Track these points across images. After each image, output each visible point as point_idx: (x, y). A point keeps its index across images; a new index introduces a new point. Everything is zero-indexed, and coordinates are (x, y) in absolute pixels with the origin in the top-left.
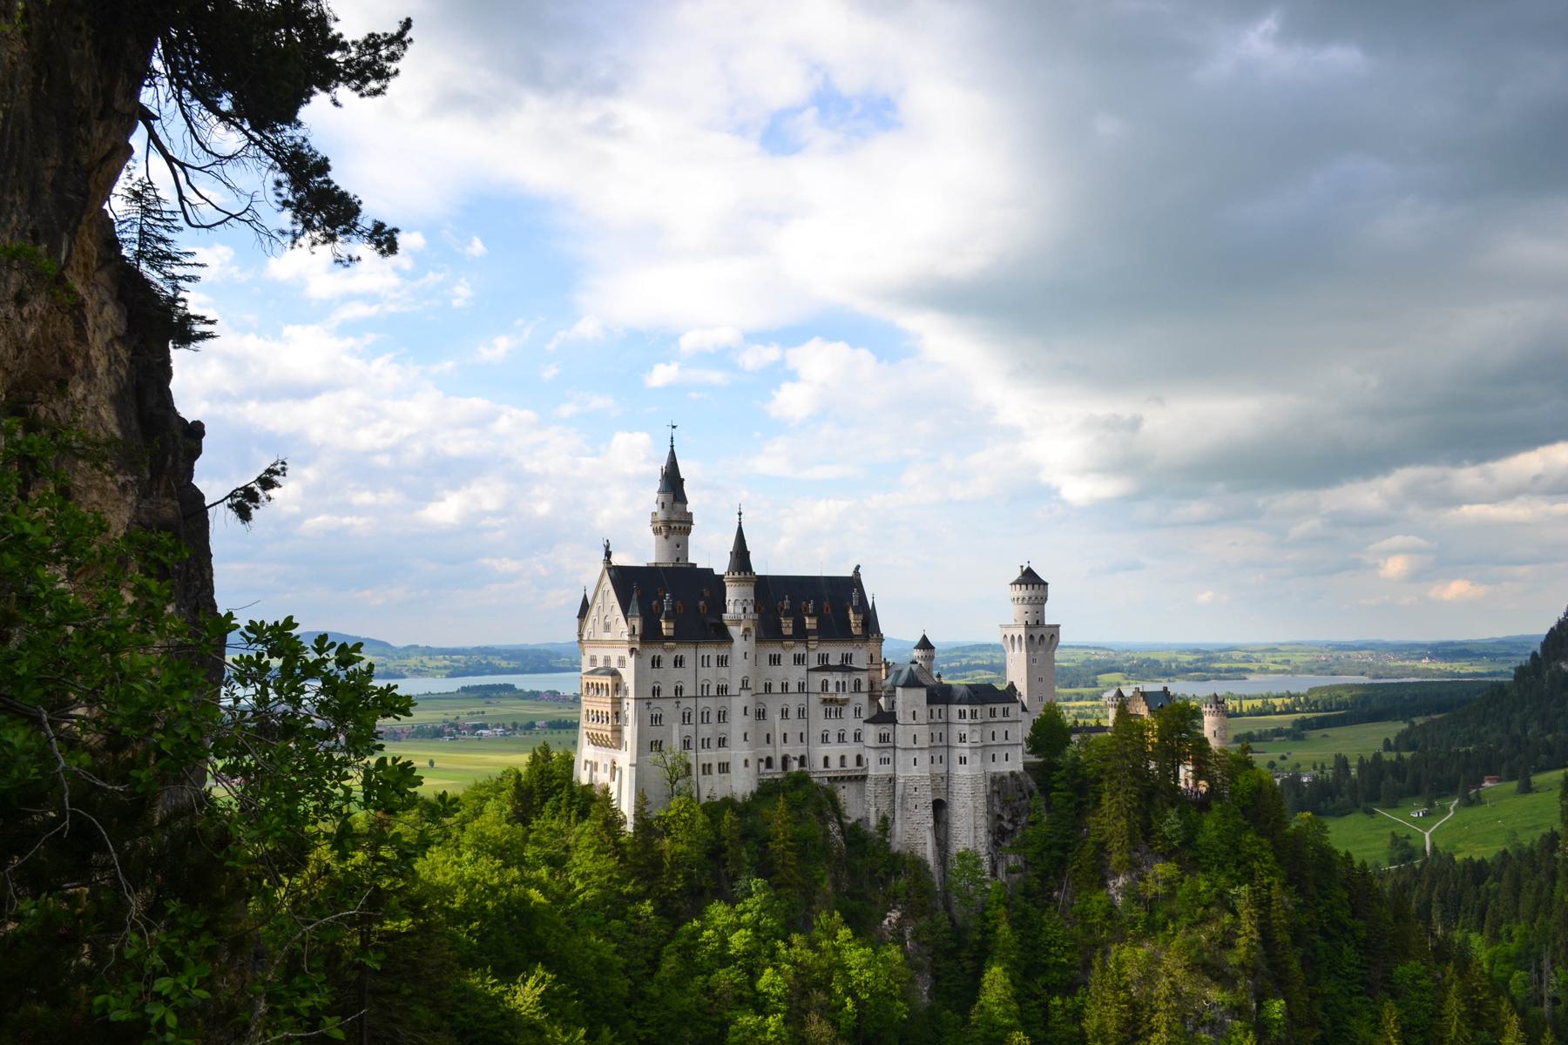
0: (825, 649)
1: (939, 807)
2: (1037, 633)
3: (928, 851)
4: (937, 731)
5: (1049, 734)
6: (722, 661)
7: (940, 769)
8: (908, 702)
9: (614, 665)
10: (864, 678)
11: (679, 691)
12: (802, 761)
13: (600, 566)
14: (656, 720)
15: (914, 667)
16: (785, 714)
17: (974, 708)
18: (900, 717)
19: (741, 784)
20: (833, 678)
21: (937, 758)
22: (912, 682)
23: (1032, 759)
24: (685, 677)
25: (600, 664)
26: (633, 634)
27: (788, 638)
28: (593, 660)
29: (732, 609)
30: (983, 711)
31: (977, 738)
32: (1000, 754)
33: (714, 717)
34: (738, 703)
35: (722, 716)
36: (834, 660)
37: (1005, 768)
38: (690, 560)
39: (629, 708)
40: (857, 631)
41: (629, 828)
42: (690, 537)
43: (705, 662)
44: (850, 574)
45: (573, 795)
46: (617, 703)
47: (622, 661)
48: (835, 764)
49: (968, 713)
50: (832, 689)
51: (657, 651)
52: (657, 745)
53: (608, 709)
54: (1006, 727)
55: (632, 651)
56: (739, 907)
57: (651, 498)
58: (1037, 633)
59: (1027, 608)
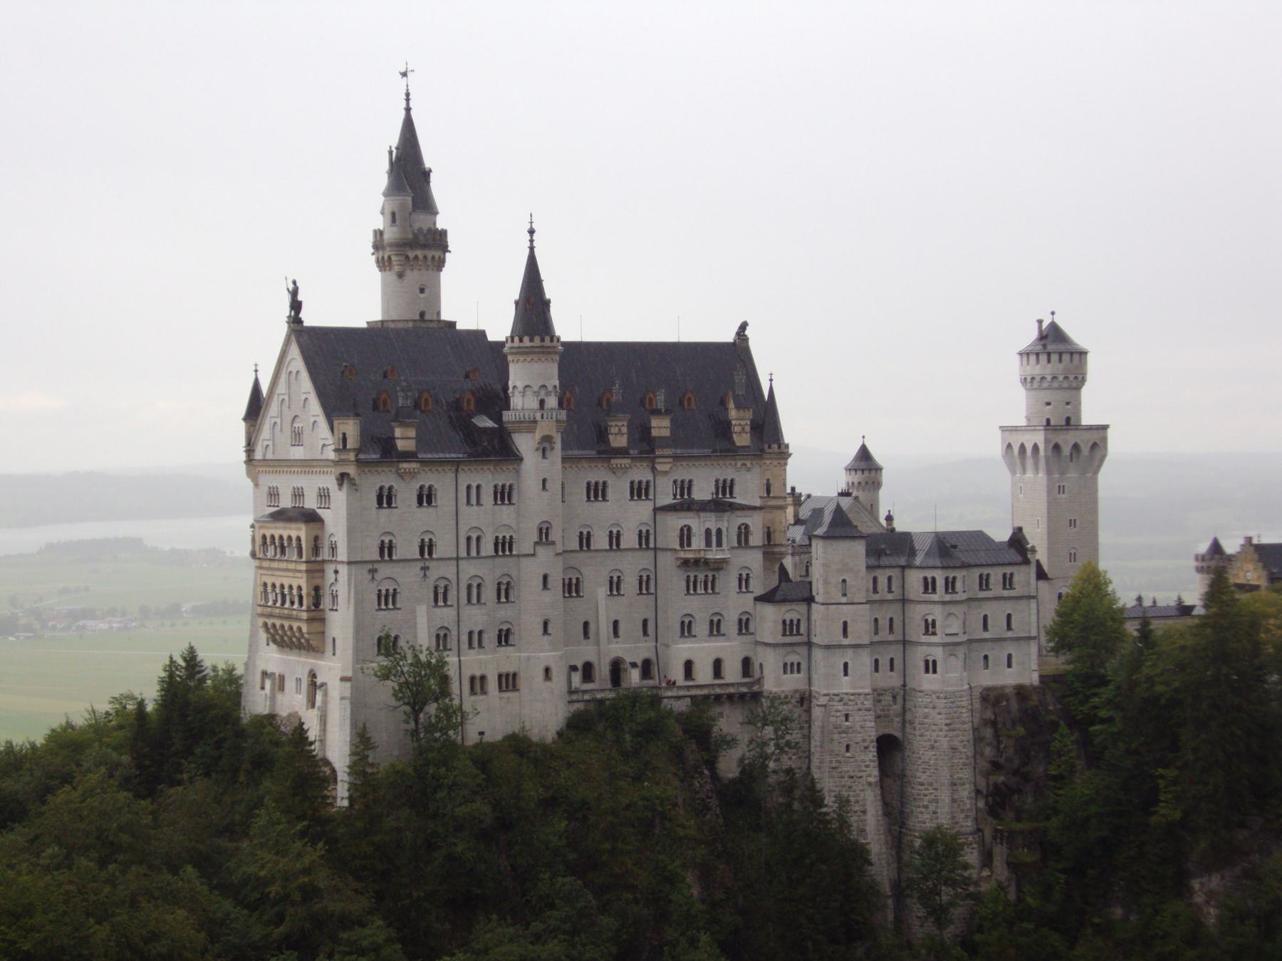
0: (683, 473)
1: (888, 747)
2: (1066, 441)
4: (884, 615)
5: (1088, 620)
6: (504, 495)
8: (834, 566)
9: (310, 503)
10: (756, 523)
11: (427, 548)
12: (646, 668)
13: (282, 329)
14: (387, 599)
15: (846, 503)
16: (615, 586)
17: (951, 574)
18: (819, 591)
19: (542, 711)
20: (699, 524)
21: (884, 663)
23: (1059, 663)
24: (437, 522)
25: (286, 502)
26: (343, 447)
27: (622, 452)
28: (273, 494)
29: (521, 403)
30: (967, 581)
31: (955, 627)
32: (998, 654)
33: (489, 594)
35: (505, 591)
36: (703, 492)
38: (445, 316)
39: (341, 582)
40: (742, 439)
41: (341, 794)
42: (446, 276)
43: (473, 496)
44: (728, 336)
45: (240, 733)
46: (316, 568)
47: (324, 495)
48: (704, 674)
49: (940, 583)
50: (698, 542)
51: (386, 478)
52: (387, 645)
53: (302, 581)
54: (1008, 607)
55: (342, 478)
56: (536, 926)
57: (368, 205)
58: (1066, 441)
59: (1047, 395)
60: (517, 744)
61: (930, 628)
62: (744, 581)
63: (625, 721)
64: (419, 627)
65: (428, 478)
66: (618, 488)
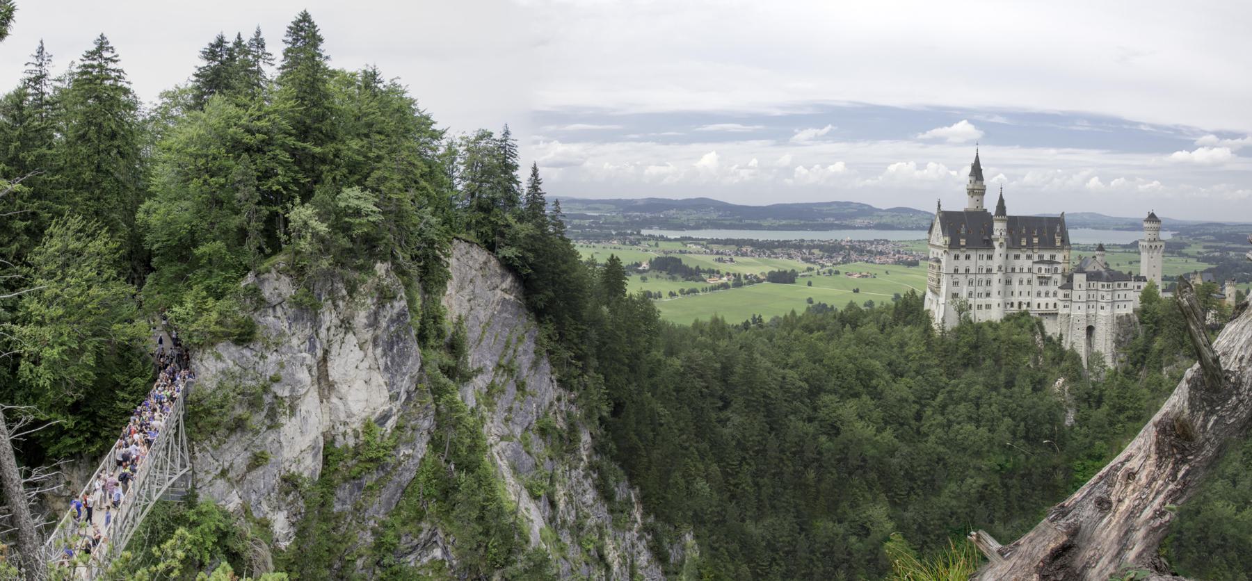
0: (1041, 253)
1: (1090, 330)
3: (1082, 350)
6: (990, 257)
7: (1092, 311)
10: (1060, 268)
11: (967, 271)
14: (956, 283)
16: (1021, 282)
20: (1044, 267)
22: (1080, 270)
29: (996, 234)
31: (1109, 297)
32: (1122, 305)
34: (996, 277)
35: (989, 282)
36: (1047, 257)
37: (1123, 312)
40: (1058, 244)
41: (938, 333)
43: (981, 257)
46: (939, 274)
48: (1043, 307)
51: (957, 252)
52: (955, 295)
60: (990, 324)
61: (1103, 297)
62: (1056, 283)
63: (1020, 319)
64: (964, 291)
65: (968, 253)
66: (1023, 256)
